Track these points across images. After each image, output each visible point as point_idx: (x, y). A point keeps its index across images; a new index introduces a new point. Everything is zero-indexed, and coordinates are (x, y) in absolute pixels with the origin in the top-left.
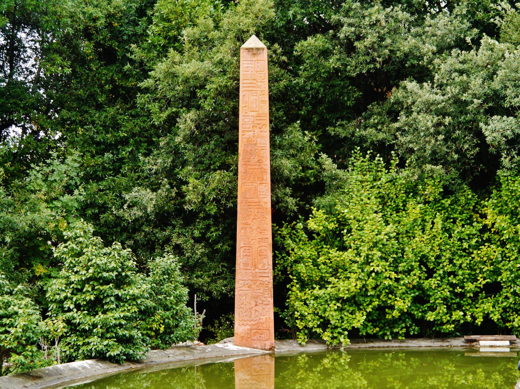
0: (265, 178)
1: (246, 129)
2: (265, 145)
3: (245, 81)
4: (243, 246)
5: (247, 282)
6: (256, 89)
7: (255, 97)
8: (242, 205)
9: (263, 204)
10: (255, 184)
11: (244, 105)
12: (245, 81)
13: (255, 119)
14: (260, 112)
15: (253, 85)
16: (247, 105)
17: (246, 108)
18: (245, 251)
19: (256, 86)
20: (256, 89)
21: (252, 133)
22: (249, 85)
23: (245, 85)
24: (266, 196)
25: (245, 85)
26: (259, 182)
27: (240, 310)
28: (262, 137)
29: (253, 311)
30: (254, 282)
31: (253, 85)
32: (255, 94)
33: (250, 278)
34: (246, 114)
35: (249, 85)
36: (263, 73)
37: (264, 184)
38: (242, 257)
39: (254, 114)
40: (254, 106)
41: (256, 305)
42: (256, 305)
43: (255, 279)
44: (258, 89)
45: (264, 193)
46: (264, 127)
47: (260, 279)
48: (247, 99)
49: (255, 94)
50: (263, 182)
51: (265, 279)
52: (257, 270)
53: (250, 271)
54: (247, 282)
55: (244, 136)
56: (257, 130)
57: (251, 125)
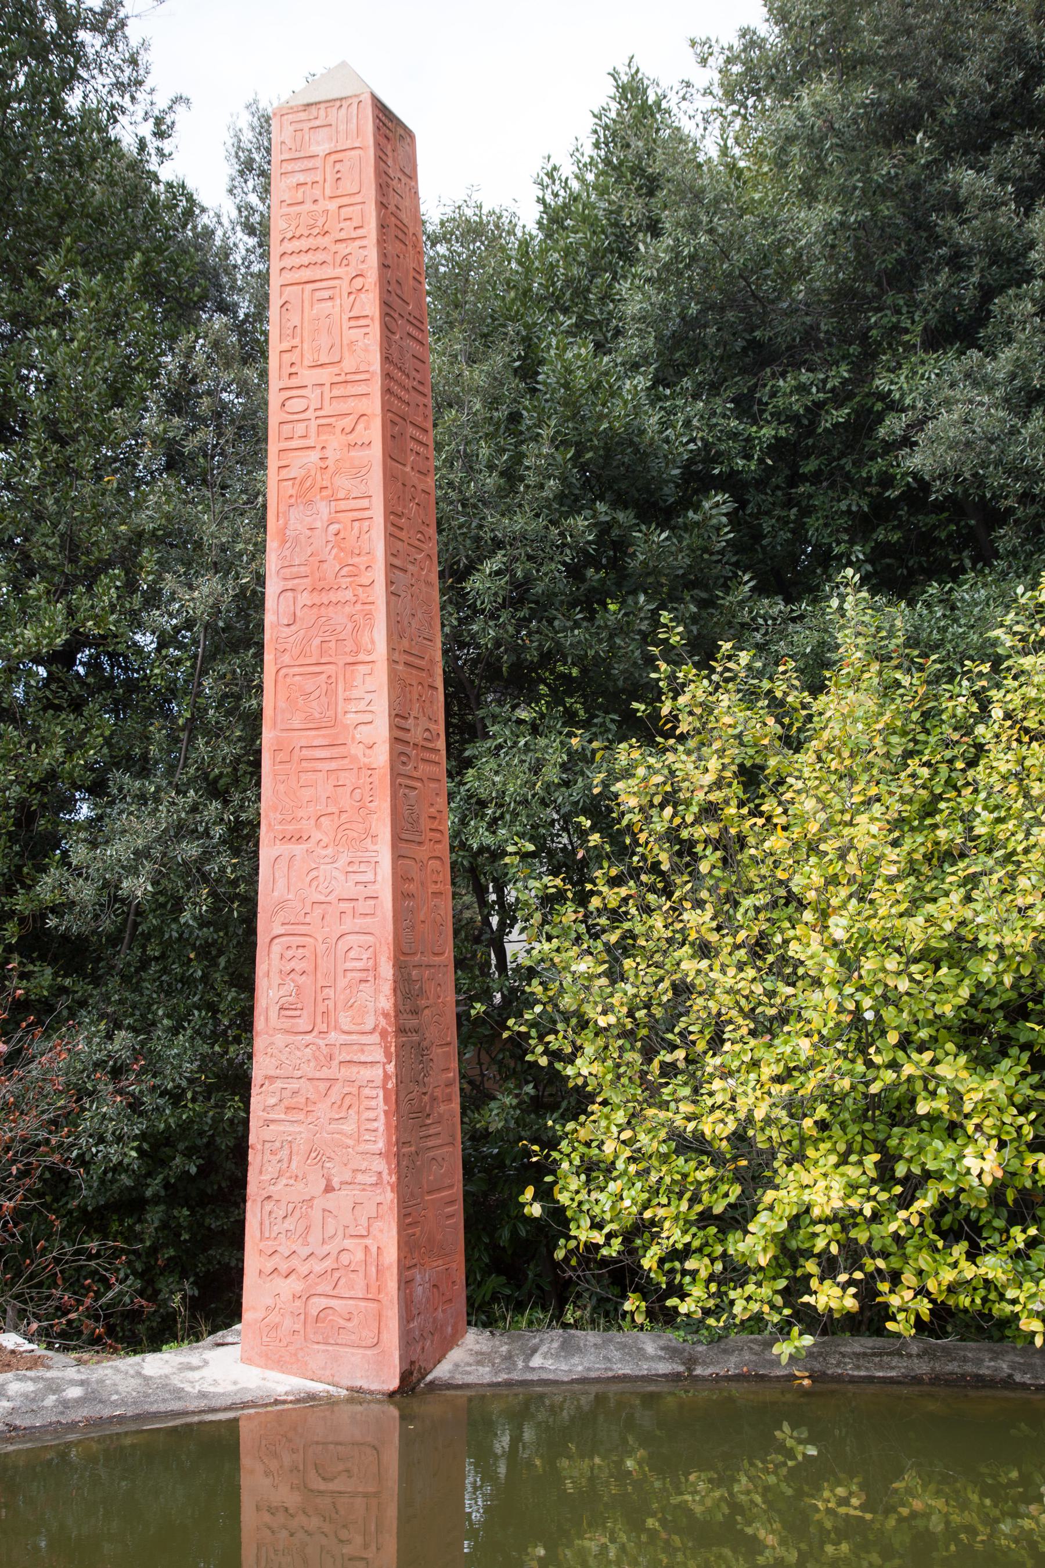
0: (366, 639)
1: (293, 444)
2: (365, 503)
3: (289, 247)
4: (281, 930)
5: (294, 1085)
6: (329, 272)
7: (330, 304)
8: (281, 756)
9: (356, 750)
10: (330, 669)
11: (286, 346)
12: (289, 247)
13: (327, 396)
14: (348, 365)
15: (320, 257)
16: (296, 342)
17: (294, 357)
18: (289, 954)
19: (329, 258)
20: (329, 272)
21: (314, 456)
22: (305, 259)
23: (288, 262)
24: (368, 718)
25: (288, 262)
26: (342, 660)
27: (269, 1206)
28: (359, 473)
29: (316, 1214)
30: (323, 1086)
31: (320, 257)
32: (326, 294)
33: (309, 1070)
34: (294, 382)
35: (305, 259)
36: (358, 199)
37: (362, 669)
38: (276, 980)
39: (324, 375)
40: (324, 341)
41: (329, 1189)
42: (329, 1189)
43: (325, 1073)
44: (339, 271)
45: (362, 705)
46: (360, 427)
47: (346, 1072)
48: (296, 320)
49: (326, 294)
50: (362, 657)
51: (366, 1073)
52: (333, 1036)
53: (308, 1038)
54: (294, 1085)
55: (284, 474)
56: (335, 443)
57: (313, 424)
